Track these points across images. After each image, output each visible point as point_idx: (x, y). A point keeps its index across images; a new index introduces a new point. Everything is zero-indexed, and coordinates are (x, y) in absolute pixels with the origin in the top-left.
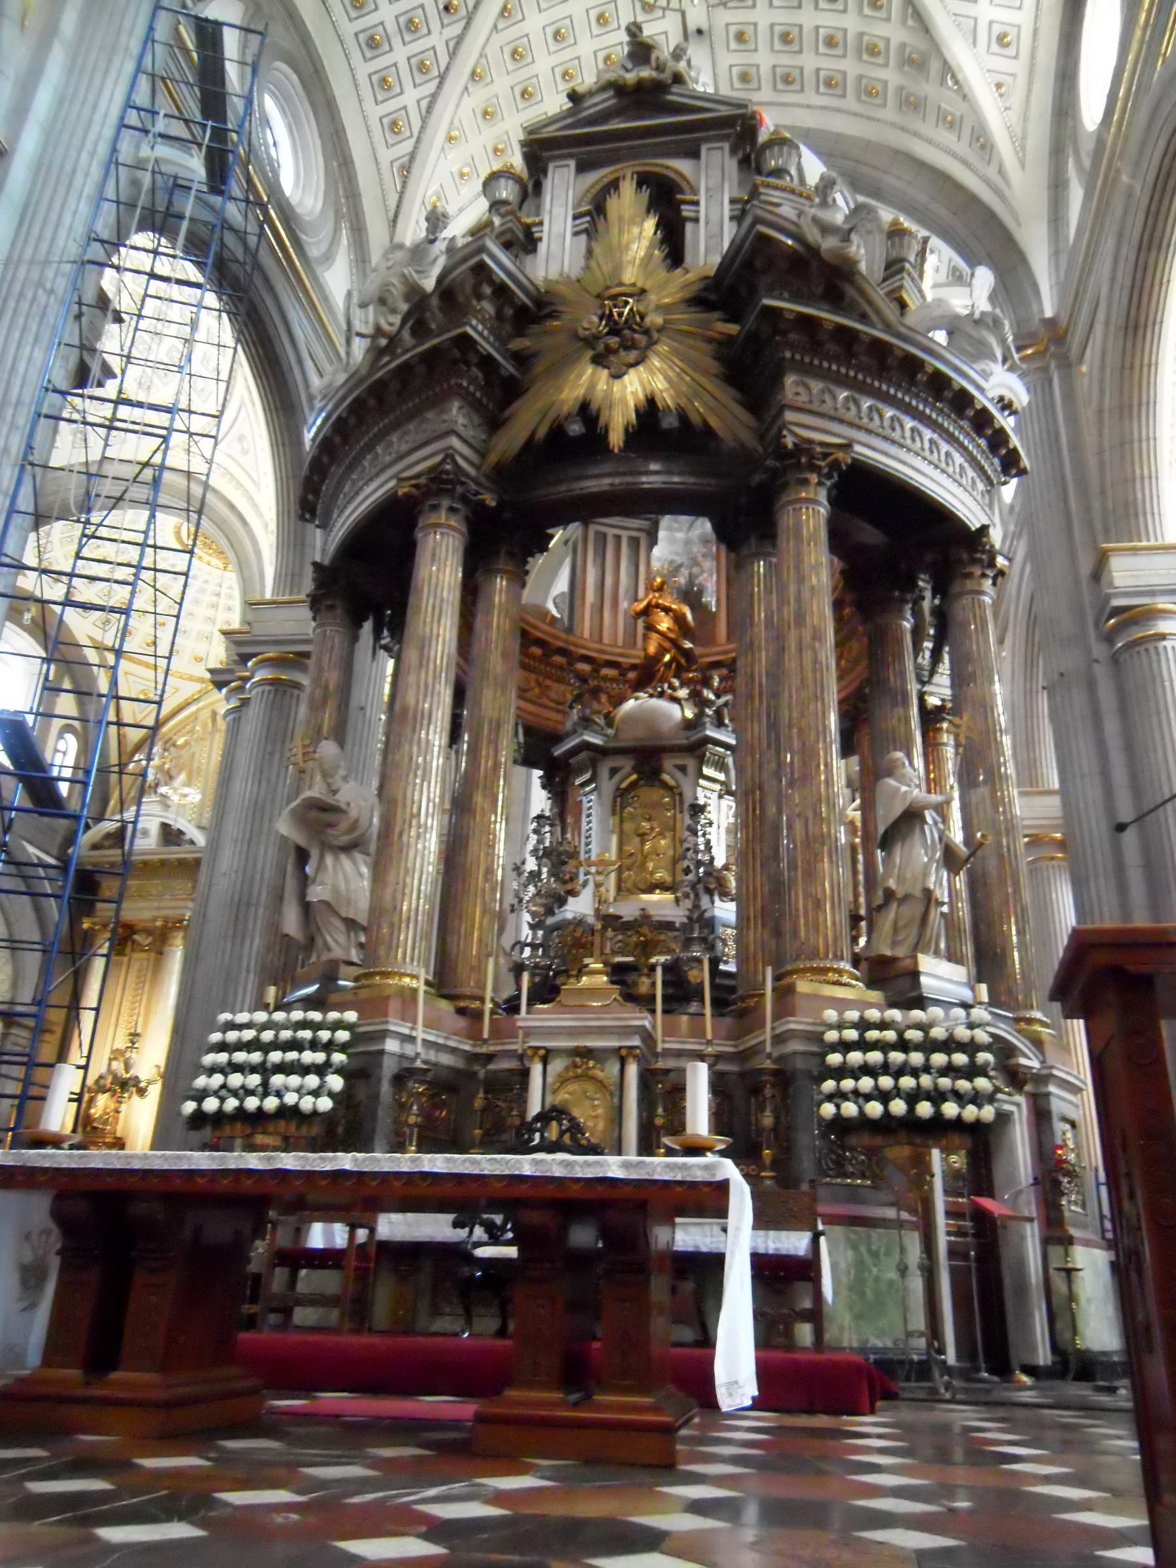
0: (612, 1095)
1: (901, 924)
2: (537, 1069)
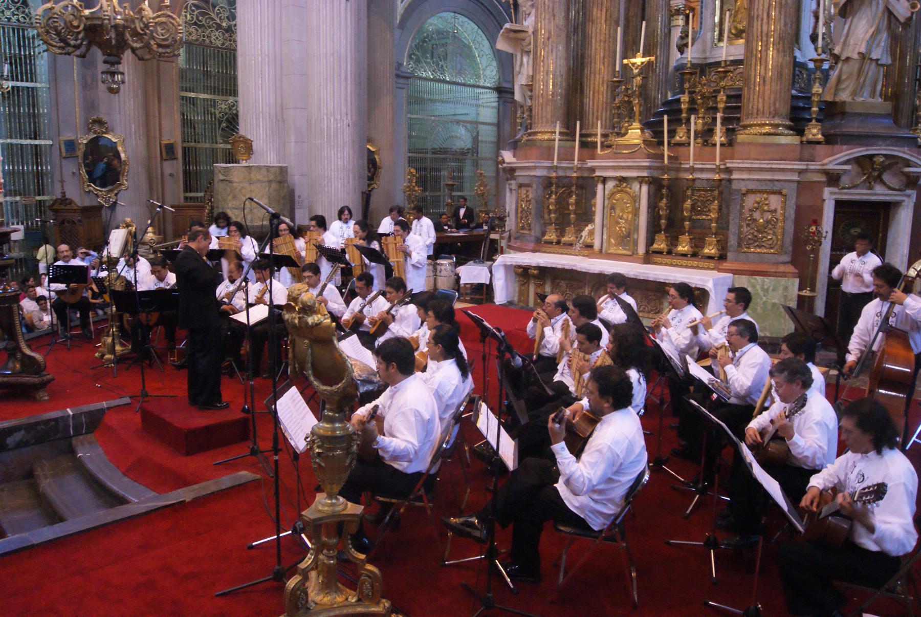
0: (635, 201)
1: (844, 77)
2: (600, 187)
